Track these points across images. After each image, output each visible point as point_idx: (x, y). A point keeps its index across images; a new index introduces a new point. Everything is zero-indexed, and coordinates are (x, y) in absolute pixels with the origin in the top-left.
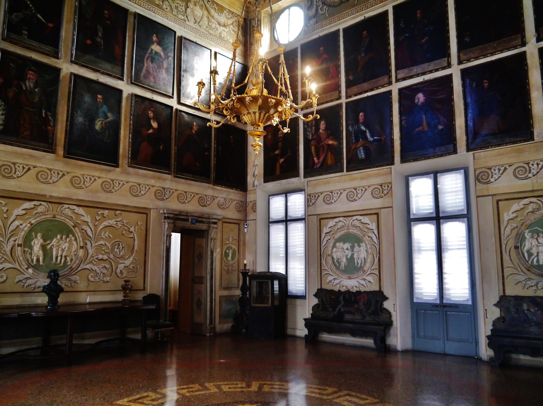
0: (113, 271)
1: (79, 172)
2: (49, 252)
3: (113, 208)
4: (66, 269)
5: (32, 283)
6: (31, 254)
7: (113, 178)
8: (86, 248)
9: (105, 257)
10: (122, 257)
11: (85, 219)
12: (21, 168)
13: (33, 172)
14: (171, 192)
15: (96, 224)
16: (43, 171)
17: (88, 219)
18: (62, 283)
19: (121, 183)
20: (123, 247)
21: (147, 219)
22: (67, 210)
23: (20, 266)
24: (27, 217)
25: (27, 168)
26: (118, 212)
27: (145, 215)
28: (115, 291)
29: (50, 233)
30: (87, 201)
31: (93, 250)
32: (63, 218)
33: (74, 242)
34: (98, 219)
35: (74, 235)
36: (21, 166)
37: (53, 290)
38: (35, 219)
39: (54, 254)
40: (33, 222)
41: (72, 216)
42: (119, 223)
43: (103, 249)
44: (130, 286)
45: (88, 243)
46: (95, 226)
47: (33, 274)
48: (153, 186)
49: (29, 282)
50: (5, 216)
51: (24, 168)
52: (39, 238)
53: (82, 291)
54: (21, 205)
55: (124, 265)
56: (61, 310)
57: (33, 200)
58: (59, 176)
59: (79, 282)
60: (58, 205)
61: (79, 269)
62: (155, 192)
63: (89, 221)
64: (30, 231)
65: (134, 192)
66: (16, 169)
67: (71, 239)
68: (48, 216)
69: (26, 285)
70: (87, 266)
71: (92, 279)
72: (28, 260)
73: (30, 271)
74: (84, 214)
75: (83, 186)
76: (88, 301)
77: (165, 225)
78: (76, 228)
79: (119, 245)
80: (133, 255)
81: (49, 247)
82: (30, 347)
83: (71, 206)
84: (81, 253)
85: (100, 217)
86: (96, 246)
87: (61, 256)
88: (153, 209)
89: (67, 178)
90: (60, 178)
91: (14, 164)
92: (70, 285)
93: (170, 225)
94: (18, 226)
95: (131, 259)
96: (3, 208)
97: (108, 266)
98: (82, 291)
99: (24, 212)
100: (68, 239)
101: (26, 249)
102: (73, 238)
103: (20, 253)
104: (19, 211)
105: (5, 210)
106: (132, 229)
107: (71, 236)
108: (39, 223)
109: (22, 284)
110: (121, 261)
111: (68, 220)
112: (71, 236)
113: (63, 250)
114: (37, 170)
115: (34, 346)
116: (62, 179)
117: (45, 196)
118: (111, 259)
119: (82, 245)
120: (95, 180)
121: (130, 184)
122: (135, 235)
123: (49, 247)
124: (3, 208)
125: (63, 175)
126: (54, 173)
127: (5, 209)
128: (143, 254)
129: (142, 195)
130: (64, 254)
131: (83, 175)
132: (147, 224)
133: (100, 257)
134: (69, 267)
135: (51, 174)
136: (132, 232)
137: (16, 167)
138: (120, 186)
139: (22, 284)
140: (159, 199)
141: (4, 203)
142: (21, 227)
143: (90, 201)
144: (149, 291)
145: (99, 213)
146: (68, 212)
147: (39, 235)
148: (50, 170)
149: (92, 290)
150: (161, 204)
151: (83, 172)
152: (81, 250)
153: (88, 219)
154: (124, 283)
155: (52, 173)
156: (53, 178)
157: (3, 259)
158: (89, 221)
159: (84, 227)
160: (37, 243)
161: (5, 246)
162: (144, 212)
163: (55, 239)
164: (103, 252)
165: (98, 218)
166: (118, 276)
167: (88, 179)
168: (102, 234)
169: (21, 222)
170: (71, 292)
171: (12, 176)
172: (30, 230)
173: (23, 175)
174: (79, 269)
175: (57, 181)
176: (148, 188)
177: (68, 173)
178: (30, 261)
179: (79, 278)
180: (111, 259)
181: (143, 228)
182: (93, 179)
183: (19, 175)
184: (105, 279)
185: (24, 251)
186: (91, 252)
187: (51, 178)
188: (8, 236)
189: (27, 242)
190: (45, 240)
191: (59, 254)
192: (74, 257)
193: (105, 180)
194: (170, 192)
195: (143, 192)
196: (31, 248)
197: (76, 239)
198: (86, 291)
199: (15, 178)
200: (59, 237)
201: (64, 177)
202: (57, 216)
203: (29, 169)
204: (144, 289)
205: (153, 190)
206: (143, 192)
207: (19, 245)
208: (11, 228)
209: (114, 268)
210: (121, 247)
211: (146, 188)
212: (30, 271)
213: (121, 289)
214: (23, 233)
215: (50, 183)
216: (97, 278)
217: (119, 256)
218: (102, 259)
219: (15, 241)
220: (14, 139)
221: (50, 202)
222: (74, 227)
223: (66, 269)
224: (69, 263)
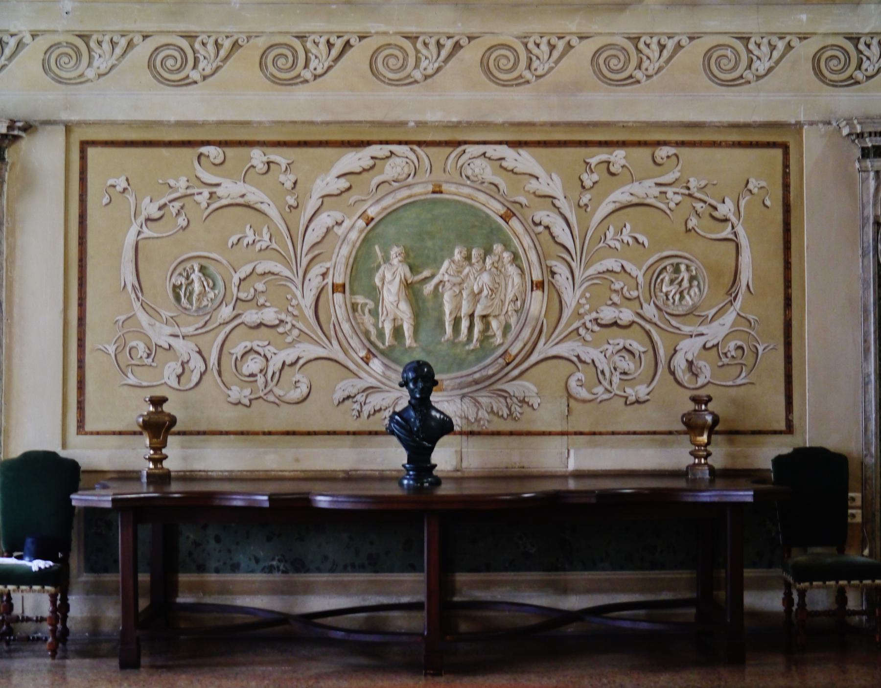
0: (658, 365)
1: (508, 31)
2: (430, 304)
3: (643, 140)
4: (488, 361)
5: (384, 404)
6: (374, 313)
7: (634, 30)
8: (551, 284)
9: (626, 315)
10: (690, 314)
11: (544, 189)
12: (323, 47)
13: (359, 54)
15: (585, 200)
16: (389, 45)
17: (552, 185)
18: (444, 402)
19: (671, 44)
20: (692, 278)
21: (786, 165)
22: (478, 162)
23: (346, 352)
24: (353, 197)
25: (339, 44)
26: (663, 152)
27: (778, 153)
28: (670, 433)
29: (429, 244)
30: (544, 124)
31: (578, 293)
32: (466, 191)
33: (512, 270)
34: (588, 183)
35: (507, 246)
36: (323, 40)
37: (420, 429)
38: (378, 201)
39: (447, 309)
40: (371, 212)
41: (497, 180)
42: (670, 191)
43: (617, 286)
44: (709, 418)
45: (561, 269)
47: (384, 375)
48: (803, 37)
49: (376, 401)
50: (291, 201)
52: (395, 261)
53: (550, 434)
54: (332, 164)
55: (701, 341)
56: (446, 489)
57: (369, 143)
58: (444, 53)
59: (535, 401)
60: (448, 150)
61: (534, 358)
62: (816, 60)
63: (558, 192)
64: (367, 241)
65: (725, 68)
66: (307, 52)
67: (500, 258)
69: (367, 409)
70: (564, 349)
71: (583, 394)
72: (367, 334)
73: (376, 365)
74: (538, 170)
75: (528, 75)
76: (572, 466)
77: (865, 181)
78: (514, 222)
79: (677, 269)
80: (738, 304)
81: (428, 288)
82: (393, 600)
83: (490, 150)
85: (595, 177)
86: (590, 278)
87: (472, 316)
88: (811, 123)
89: (471, 54)
90: (450, 55)
91: (301, 37)
92: (505, 412)
94: (328, 230)
95: (730, 317)
96: (282, 178)
97: (637, 347)
98: (550, 434)
99: (343, 184)
100: (489, 261)
101: (360, 299)
102: (507, 256)
103: (341, 313)
105: (289, 185)
106: (726, 209)
107: (498, 248)
108: (392, 214)
109: (357, 407)
110: (686, 329)
111: (482, 197)
112: (498, 248)
113: (476, 297)
114: (371, 44)
115: (405, 600)
116: (451, 64)
117: (404, 124)
118: (649, 322)
119: (537, 276)
120: (569, 46)
121: (708, 42)
122: (740, 229)
123: (428, 288)
124: (282, 178)
125: (457, 46)
126: (426, 44)
128: (781, 298)
129: (759, 78)
130: (479, 311)
131: (524, 39)
132: (786, 186)
133: (608, 314)
134: (501, 351)
135: (417, 51)
136: (726, 220)
137: (309, 45)
138: (666, 54)
139: (357, 407)
140: (834, 84)
141: (283, 162)
142: (340, 231)
143: (554, 125)
144: (810, 435)
145: (593, 161)
146: (483, 170)
147: (394, 251)
148: (413, 38)
149: (587, 430)
150: (846, 102)
151: (520, 29)
152: (537, 294)
153: (554, 186)
154: (691, 406)
155: (419, 45)
156: (424, 64)
157: (296, 332)
158: (558, 192)
159: (539, 216)
160: (391, 277)
161: (299, 294)
162: (775, 140)
163: (446, 264)
164: (616, 298)
166: (676, 380)
167: (544, 47)
168: (610, 234)
169: (339, 216)
170: (511, 433)
171: (299, 76)
172: (364, 240)
173: (330, 68)
174: (534, 358)
175: (439, 69)
176: (781, 45)
177: (470, 38)
178: (373, 338)
179: (534, 389)
180: (649, 322)
181: (774, 201)
182: (561, 45)
183: (320, 71)
184: (629, 391)
185: (354, 307)
186: (570, 298)
187: (417, 66)
188: (305, 261)
189: (360, 276)
190: (413, 269)
191: (465, 310)
192: (513, 321)
195: (761, 67)
196: (374, 293)
197: (515, 258)
198: (562, 434)
199: (306, 81)
200: (458, 254)
201: (461, 54)
202: (445, 187)
203: (347, 45)
204: (790, 429)
205: (806, 50)
206: (761, 67)
207: (335, 288)
208: (312, 237)
209: (661, 352)
210: (685, 275)
211: (773, 48)
212: (376, 365)
213: (683, 428)
214: (345, 250)
215: (416, 82)
216: (600, 390)
217: (680, 310)
218: (615, 324)
219: (324, 275)
221: (420, 144)
222: (506, 218)
223: (488, 361)
224: (498, 340)
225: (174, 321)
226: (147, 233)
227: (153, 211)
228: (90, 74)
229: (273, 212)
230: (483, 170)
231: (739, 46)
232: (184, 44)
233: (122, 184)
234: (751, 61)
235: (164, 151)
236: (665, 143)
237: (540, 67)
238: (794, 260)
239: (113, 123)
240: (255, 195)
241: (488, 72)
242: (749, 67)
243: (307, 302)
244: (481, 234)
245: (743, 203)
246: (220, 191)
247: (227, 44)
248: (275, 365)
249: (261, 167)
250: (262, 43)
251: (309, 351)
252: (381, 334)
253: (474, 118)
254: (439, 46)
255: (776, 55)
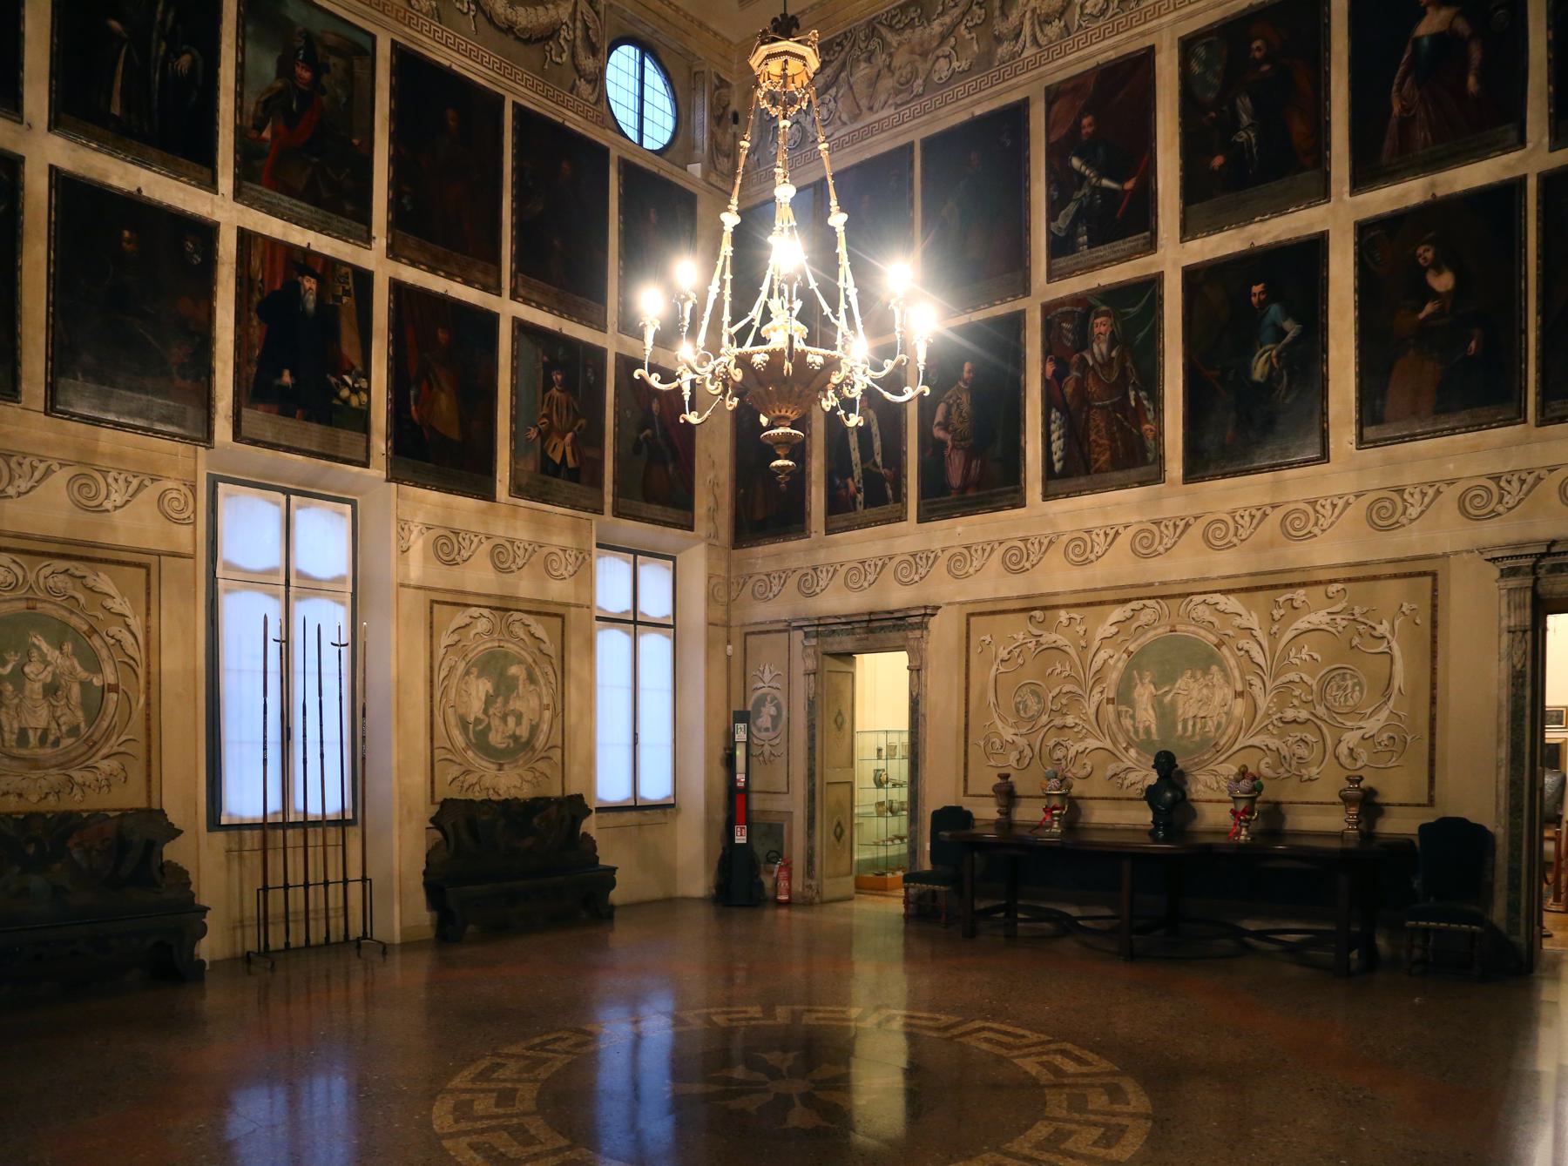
1: (1221, 510)
11: (1246, 624)
12: (1102, 536)
14: (1530, 479)
15: (1274, 629)
17: (1253, 621)
19: (1341, 503)
21: (1434, 590)
24: (1120, 638)
25: (1112, 533)
27: (1428, 580)
32: (1192, 629)
34: (1277, 617)
40: (1131, 648)
42: (1338, 617)
43: (1297, 693)
45: (1257, 682)
46: (1272, 636)
48: (1451, 482)
51: (1106, 535)
63: (1255, 626)
64: (1128, 668)
68: (1160, 630)
74: (1241, 610)
75: (1235, 540)
78: (1224, 649)
81: (1168, 699)
84: (1239, 707)
85: (1282, 612)
88: (1456, 553)
89: (1196, 530)
90: (1183, 532)
93: (1517, 597)
99: (1114, 629)
101: (1123, 708)
103: (1112, 717)
104: (1106, 629)
111: (1203, 632)
114: (1132, 531)
117: (1151, 585)
119: (1239, 687)
120: (1265, 515)
122: (1394, 645)
123: (1168, 699)
125: (1187, 525)
127: (1081, 629)
129: (1412, 521)
131: (1232, 513)
132: (1434, 607)
138: (1337, 511)
140: (1477, 518)
141: (1078, 617)
142: (1111, 662)
145: (1281, 600)
146: (1203, 612)
148: (1157, 523)
152: (1240, 700)
153: (1253, 621)
159: (1242, 643)
165: (1277, 614)
167: (1247, 518)
169: (1111, 652)
176: (1431, 492)
181: (1423, 620)
182: (1258, 514)
186: (1263, 703)
193: (1292, 507)
194: (1523, 482)
195: (1413, 512)
196: (1131, 703)
202: (1178, 627)
207: (1110, 701)
211: (1424, 494)
220: (1082, 480)
221: (1162, 597)
222: (1218, 646)
225: (1015, 725)
226: (1002, 669)
227: (1003, 654)
228: (971, 570)
229: (1072, 651)
230: (1203, 612)
231: (1395, 496)
232: (1021, 545)
233: (988, 639)
234: (1405, 508)
235: (1011, 616)
236: (1336, 581)
237: (1243, 533)
238: (1439, 667)
239: (984, 601)
240: (1062, 641)
241: (1207, 541)
242: (1404, 513)
243: (1092, 711)
244: (1203, 659)
245: (1397, 623)
246: (1042, 640)
247: (1046, 542)
248: (1072, 753)
249: (1065, 622)
250: (1065, 539)
251: (1092, 743)
252: (1136, 732)
253: (1197, 576)
254: (1176, 526)
255: (1427, 500)
